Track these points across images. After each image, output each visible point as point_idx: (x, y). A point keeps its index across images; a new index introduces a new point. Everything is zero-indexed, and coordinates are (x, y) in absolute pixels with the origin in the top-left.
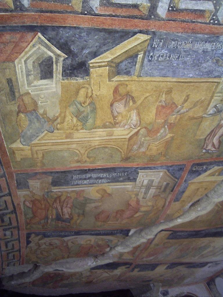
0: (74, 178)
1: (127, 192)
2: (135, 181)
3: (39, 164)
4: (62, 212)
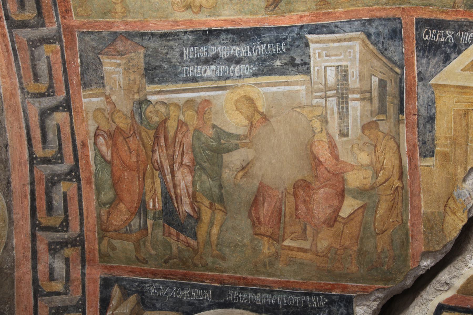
0: (185, 56)
1: (299, 107)
2: (308, 72)
3: (119, 8)
4: (175, 186)
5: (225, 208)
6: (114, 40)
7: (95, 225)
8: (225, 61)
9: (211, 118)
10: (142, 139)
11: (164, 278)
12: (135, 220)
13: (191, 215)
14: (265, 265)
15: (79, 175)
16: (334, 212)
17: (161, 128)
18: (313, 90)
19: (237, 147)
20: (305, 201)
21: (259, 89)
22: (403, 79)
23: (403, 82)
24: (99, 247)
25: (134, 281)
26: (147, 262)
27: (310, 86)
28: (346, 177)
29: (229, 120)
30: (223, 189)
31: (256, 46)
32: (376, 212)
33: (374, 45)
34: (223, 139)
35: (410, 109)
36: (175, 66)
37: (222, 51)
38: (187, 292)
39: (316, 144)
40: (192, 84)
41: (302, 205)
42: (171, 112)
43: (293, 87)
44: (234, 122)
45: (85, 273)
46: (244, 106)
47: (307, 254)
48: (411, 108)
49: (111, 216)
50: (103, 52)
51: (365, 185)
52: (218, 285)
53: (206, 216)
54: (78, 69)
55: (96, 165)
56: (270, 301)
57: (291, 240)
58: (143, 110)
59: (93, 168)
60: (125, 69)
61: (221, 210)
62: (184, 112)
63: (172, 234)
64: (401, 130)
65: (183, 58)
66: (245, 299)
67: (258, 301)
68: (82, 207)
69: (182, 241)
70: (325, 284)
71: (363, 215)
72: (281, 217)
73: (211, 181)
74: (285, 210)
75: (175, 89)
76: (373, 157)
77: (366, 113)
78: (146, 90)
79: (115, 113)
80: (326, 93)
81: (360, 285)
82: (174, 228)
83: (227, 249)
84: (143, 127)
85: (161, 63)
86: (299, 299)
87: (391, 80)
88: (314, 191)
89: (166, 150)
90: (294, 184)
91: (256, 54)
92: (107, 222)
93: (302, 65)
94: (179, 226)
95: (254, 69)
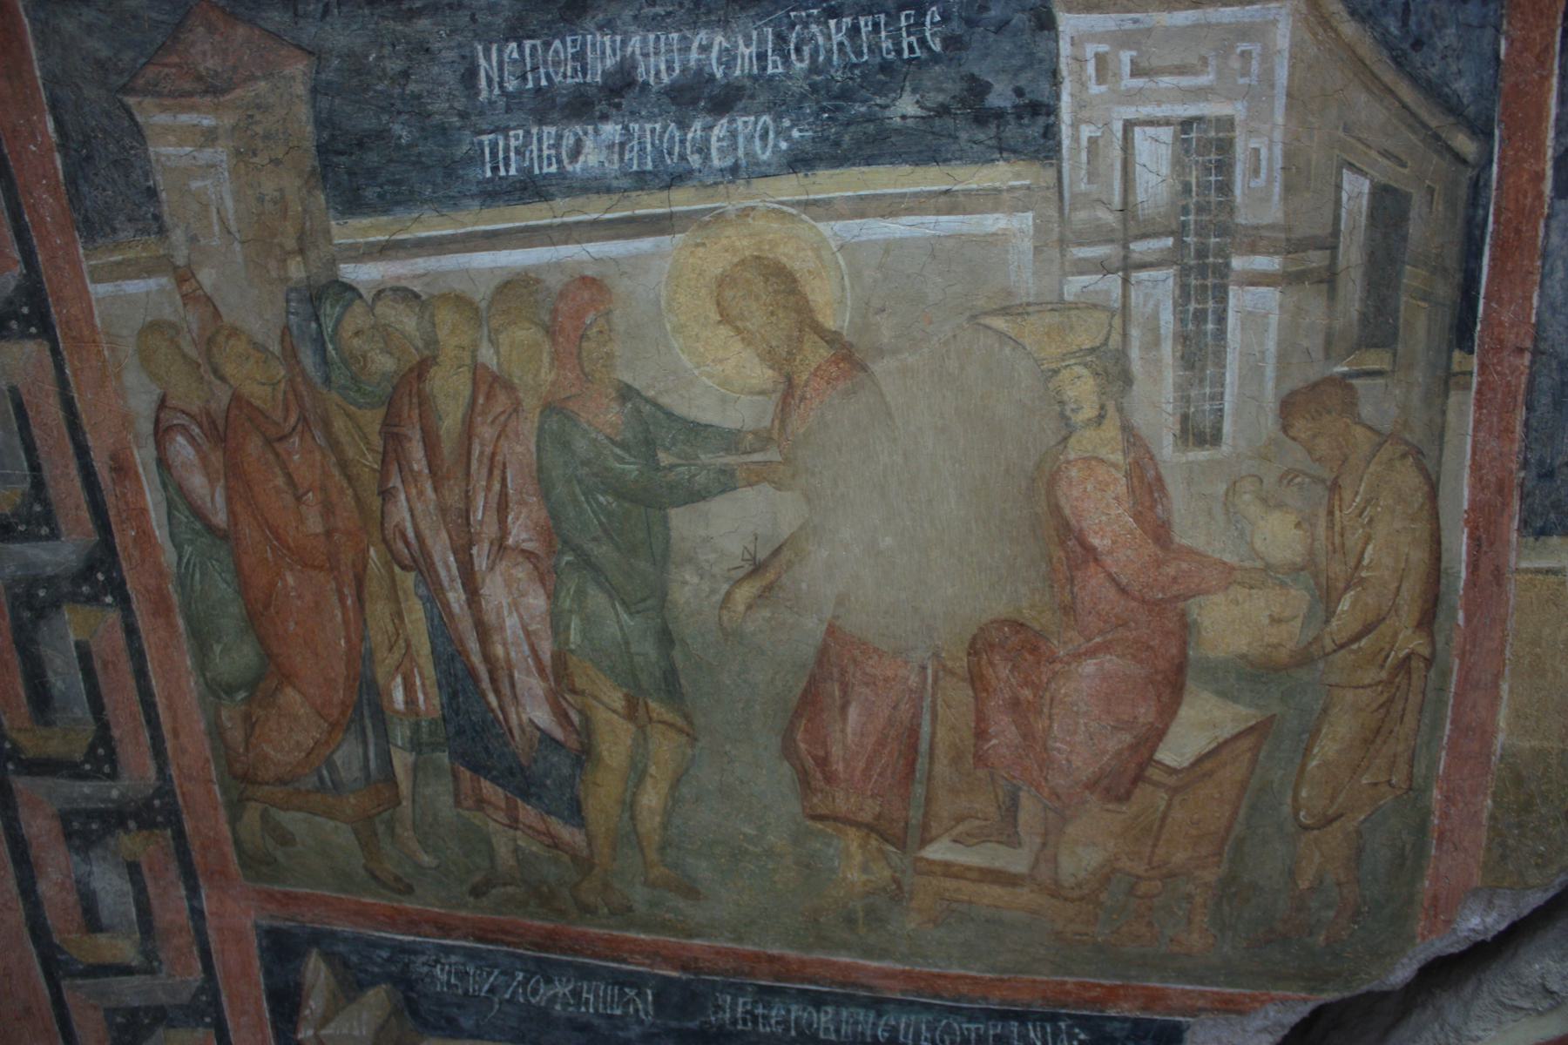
0: (483, 83)
1: (1004, 311)
2: (1046, 148)
4: (484, 632)
5: (687, 717)
6: (179, 26)
7: (207, 760)
8: (665, 100)
9: (610, 355)
10: (334, 445)
11: (479, 939)
12: (345, 748)
13: (553, 740)
14: (850, 921)
15: (123, 583)
16: (1134, 748)
17: (406, 399)
18: (1070, 236)
19: (726, 482)
20: (1015, 704)
21: (821, 226)
22: (1487, 185)
23: (1482, 201)
24: (234, 831)
25: (375, 944)
26: (409, 890)
27: (1053, 212)
28: (1194, 613)
29: (689, 365)
30: (678, 647)
31: (806, 26)
32: (1307, 752)
33: (1363, 20)
34: (667, 449)
35: (1501, 324)
36: (443, 130)
37: (646, 55)
38: (566, 991)
39: (1074, 473)
40: (521, 210)
41: (1005, 720)
42: (442, 334)
43: (975, 218)
44: (710, 376)
45: (202, 912)
46: (754, 306)
47: (1018, 890)
48: (1506, 318)
49: (257, 731)
50: (141, 81)
51: (1276, 646)
52: (674, 974)
53: (616, 744)
54: (53, 162)
55: (178, 547)
56: (869, 1032)
57: (955, 841)
58: (328, 329)
59: (169, 556)
60: (238, 153)
61: (671, 725)
62: (497, 331)
63: (490, 803)
64: (1451, 417)
65: (478, 94)
66: (778, 1023)
67: (827, 1030)
68: (152, 695)
69: (530, 827)
70: (1083, 986)
71: (1254, 761)
72: (914, 761)
73: (625, 617)
74: (933, 734)
75: (450, 232)
76: (1321, 531)
77: (1305, 343)
78: (330, 241)
79: (221, 339)
80: (1126, 247)
81: (1215, 989)
82: (494, 780)
83: (704, 864)
84: (335, 396)
85: (385, 118)
86: (978, 1029)
87: (1431, 191)
88: (1058, 666)
89: (436, 489)
90: (974, 638)
91: (805, 65)
92: (247, 749)
93: (1020, 117)
94: (512, 774)
95: (796, 134)
